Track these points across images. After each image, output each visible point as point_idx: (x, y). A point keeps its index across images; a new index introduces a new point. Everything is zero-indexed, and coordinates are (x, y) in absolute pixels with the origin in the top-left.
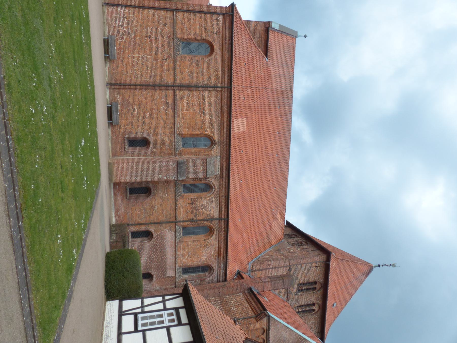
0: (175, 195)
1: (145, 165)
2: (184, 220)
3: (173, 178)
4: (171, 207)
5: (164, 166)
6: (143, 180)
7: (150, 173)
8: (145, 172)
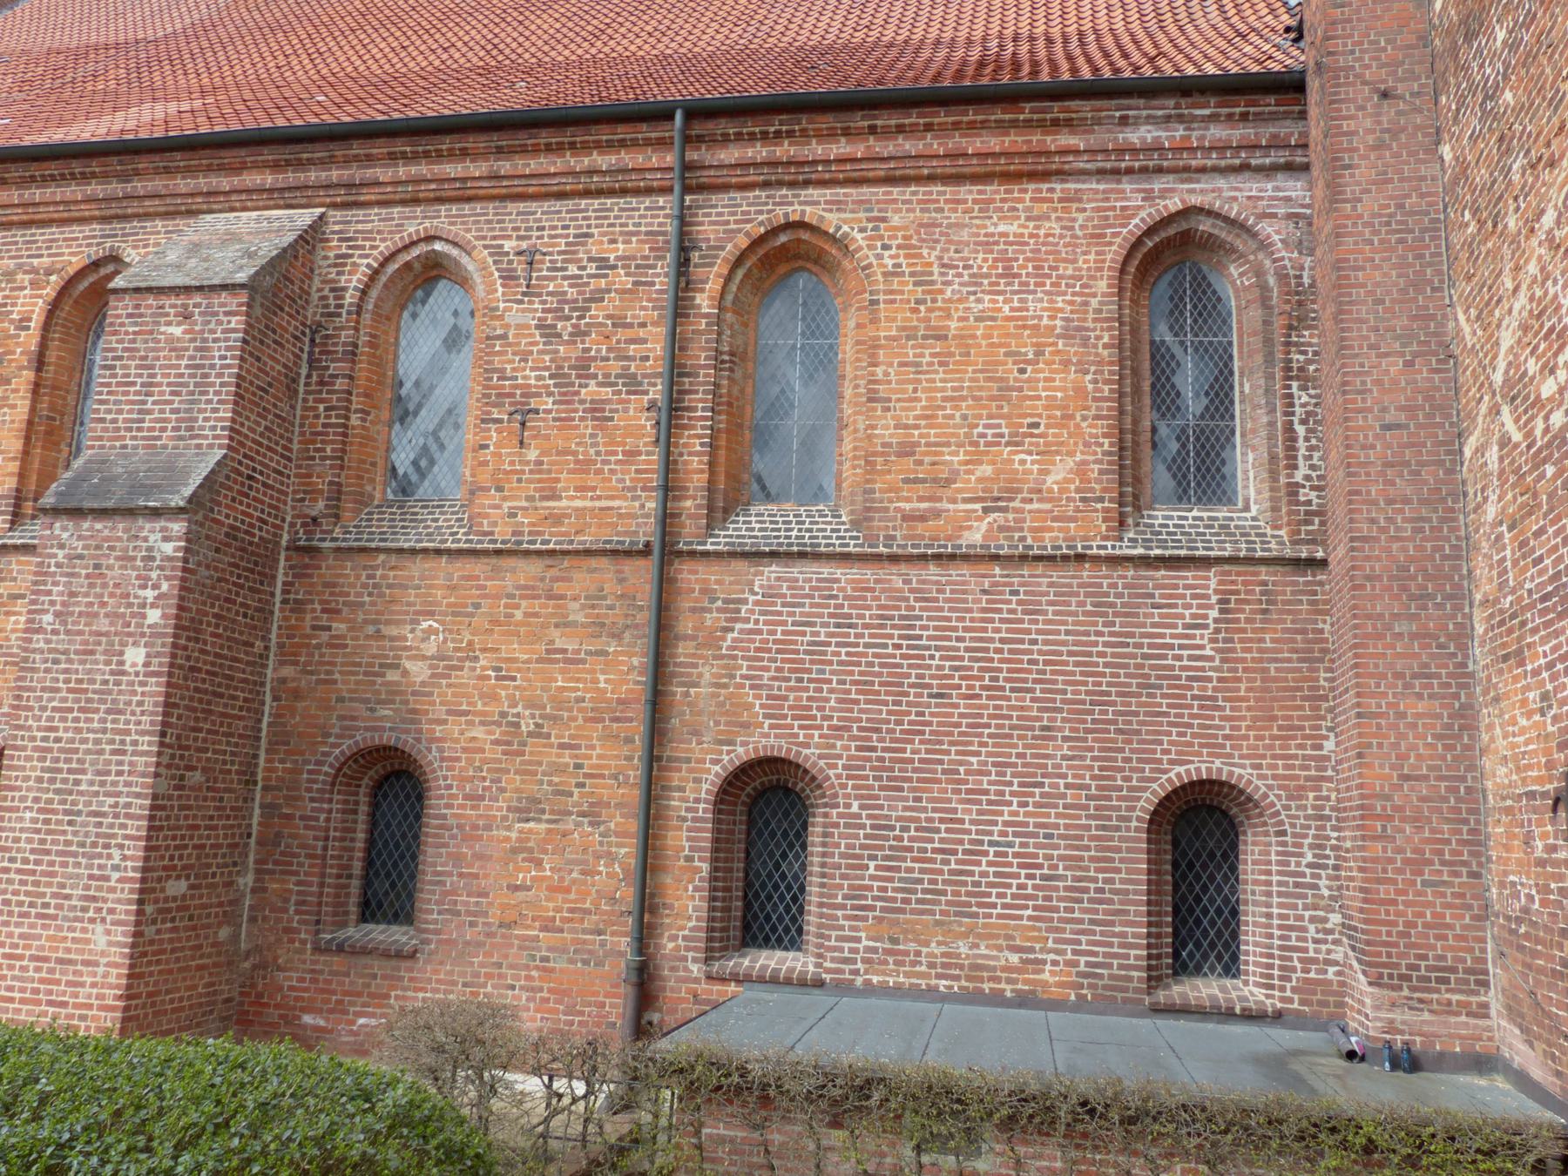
0: (438, 552)
1: (26, 779)
2: (655, 479)
3: (168, 548)
4: (529, 592)
5: (64, 623)
6: (141, 806)
7: (97, 742)
8: (77, 782)
